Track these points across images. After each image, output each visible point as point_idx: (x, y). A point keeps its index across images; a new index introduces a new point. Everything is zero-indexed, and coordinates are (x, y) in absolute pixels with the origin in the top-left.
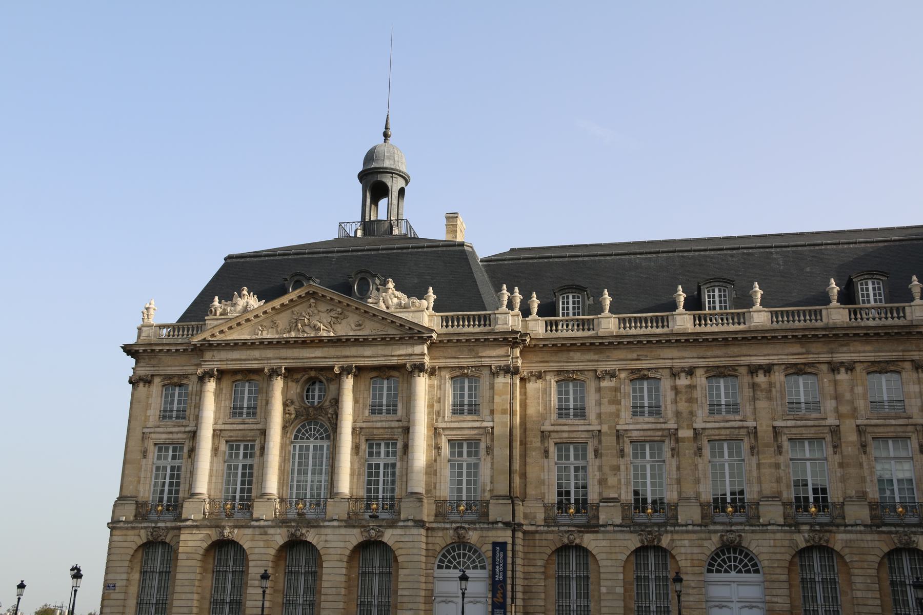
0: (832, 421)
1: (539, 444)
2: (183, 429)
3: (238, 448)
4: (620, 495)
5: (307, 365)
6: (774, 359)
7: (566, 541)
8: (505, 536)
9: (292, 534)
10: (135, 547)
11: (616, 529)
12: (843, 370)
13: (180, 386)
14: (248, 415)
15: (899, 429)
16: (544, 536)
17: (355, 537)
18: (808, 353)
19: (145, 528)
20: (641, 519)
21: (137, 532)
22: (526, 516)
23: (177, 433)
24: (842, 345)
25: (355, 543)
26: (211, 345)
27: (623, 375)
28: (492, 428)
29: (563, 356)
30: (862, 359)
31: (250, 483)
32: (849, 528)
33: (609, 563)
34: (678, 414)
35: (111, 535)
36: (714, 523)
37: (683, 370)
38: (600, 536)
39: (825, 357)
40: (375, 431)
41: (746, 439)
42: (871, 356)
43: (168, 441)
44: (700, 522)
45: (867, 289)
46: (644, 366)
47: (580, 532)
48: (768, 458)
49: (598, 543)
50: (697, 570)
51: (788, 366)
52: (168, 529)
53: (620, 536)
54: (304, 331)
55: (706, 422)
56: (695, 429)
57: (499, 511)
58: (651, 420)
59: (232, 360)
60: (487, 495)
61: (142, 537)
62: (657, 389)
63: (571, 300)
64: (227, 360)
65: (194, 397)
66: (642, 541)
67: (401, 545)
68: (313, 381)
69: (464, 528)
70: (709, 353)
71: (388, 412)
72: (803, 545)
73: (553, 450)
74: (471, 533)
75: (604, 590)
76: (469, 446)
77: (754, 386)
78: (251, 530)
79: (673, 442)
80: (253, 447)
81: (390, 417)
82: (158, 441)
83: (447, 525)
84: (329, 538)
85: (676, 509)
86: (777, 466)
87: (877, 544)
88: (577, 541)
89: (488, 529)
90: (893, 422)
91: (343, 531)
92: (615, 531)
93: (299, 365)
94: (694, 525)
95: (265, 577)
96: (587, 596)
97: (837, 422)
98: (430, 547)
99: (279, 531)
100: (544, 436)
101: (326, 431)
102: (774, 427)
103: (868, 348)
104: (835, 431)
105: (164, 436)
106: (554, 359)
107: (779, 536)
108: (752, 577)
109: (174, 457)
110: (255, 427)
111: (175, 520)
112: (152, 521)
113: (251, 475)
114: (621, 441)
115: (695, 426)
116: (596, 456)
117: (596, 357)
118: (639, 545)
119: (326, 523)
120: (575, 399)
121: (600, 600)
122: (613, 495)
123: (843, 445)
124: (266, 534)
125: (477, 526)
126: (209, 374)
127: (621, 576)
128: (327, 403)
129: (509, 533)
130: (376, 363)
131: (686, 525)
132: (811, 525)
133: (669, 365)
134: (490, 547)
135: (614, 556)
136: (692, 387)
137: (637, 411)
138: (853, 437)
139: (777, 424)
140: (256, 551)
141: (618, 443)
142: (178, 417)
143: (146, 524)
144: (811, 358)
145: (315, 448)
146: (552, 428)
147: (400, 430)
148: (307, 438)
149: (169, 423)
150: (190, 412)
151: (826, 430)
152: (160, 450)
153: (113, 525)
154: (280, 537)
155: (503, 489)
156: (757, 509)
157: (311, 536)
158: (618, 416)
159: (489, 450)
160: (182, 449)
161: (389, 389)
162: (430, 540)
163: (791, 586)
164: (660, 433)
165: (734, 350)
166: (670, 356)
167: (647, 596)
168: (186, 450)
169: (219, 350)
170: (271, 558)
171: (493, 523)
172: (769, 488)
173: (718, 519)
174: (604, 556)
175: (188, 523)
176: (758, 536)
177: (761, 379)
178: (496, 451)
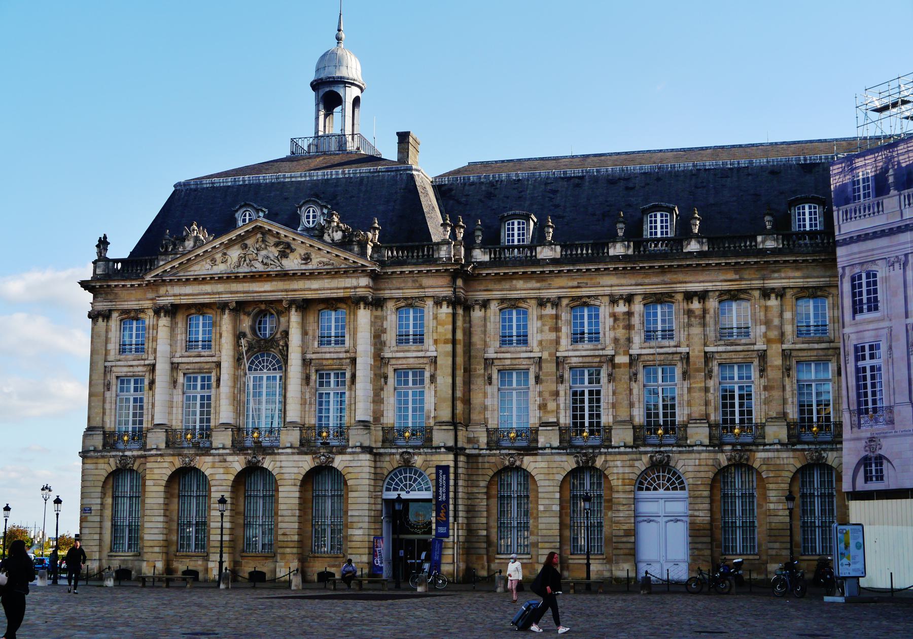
0: (760, 346)
1: (482, 371)
2: (142, 362)
3: (195, 379)
4: (558, 420)
5: (256, 299)
6: (708, 286)
7: (507, 463)
8: (448, 460)
9: (249, 462)
10: (106, 475)
11: (554, 451)
12: (773, 296)
13: (137, 319)
14: (204, 347)
15: (821, 353)
16: (486, 459)
17: (307, 463)
18: (741, 279)
19: (114, 456)
20: (579, 442)
21: (106, 460)
22: (469, 440)
23: (137, 366)
24: (774, 272)
25: (308, 469)
28: (436, 357)
29: (506, 285)
30: (791, 285)
31: (209, 413)
32: (768, 447)
33: (547, 483)
34: (616, 340)
35: (83, 463)
36: (645, 445)
37: (621, 297)
38: (539, 458)
39: (757, 283)
40: (325, 362)
41: (679, 364)
42: (800, 282)
43: (129, 374)
44: (632, 444)
45: (804, 214)
46: (584, 294)
47: (519, 454)
48: (698, 382)
49: (537, 465)
50: (628, 488)
51: (722, 293)
52: (135, 458)
53: (557, 458)
55: (641, 348)
56: (631, 355)
57: (442, 437)
58: (590, 346)
59: (186, 295)
60: (432, 422)
61: (113, 465)
62: (597, 316)
63: (516, 226)
64: (180, 295)
65: (151, 331)
66: (577, 462)
67: (350, 470)
68: (262, 314)
69: (409, 453)
70: (647, 281)
71: (337, 343)
72: (725, 463)
73: (495, 376)
74: (416, 457)
75: (541, 508)
76: (414, 375)
77: (690, 313)
79: (610, 369)
80: (209, 379)
81: (338, 348)
82: (119, 374)
83: (393, 451)
84: (283, 464)
85: (610, 432)
86: (706, 390)
87: (792, 461)
88: (518, 463)
89: (432, 454)
90: (816, 346)
91: (296, 457)
92: (552, 454)
93: (248, 297)
94: (625, 446)
95: (222, 501)
96: (526, 513)
97: (764, 347)
98: (379, 471)
99: (236, 458)
100: (489, 363)
101: (278, 362)
102: (706, 353)
103: (797, 274)
104: (763, 356)
105: (126, 369)
106: (497, 287)
107: (703, 455)
108: (679, 493)
109: (136, 390)
110: (210, 359)
111: (140, 449)
112: (119, 450)
113: (209, 406)
114: (561, 367)
115: (631, 352)
116: (537, 382)
117: (538, 285)
118: (575, 466)
119: (280, 451)
120: (518, 327)
121: (537, 518)
122: (551, 420)
123: (769, 369)
125: (422, 450)
127: (558, 495)
128: (278, 336)
129: (451, 457)
130: (322, 296)
131: (619, 447)
132: (733, 445)
133: (608, 292)
134: (434, 470)
135: (551, 477)
136: (630, 314)
137: (578, 338)
138: (778, 362)
139: (707, 349)
140: (217, 477)
141: (557, 369)
142: (137, 350)
143: (114, 453)
144: (744, 285)
145: (268, 378)
146: (494, 356)
147: (348, 361)
148: (261, 370)
149: (130, 357)
150: (148, 346)
151: (755, 355)
152: (122, 382)
153: (84, 454)
155: (446, 415)
156: (685, 431)
157: (268, 463)
158: (558, 342)
159: (433, 378)
160: (142, 381)
161: (337, 320)
162: (379, 464)
163: (712, 503)
164: (598, 360)
165: (668, 277)
166: (609, 283)
168: (146, 382)
169: (172, 286)
170: (230, 483)
171: (436, 448)
172: (698, 410)
173: (651, 441)
174: (542, 477)
176: (685, 456)
177: (696, 305)
178: (440, 380)
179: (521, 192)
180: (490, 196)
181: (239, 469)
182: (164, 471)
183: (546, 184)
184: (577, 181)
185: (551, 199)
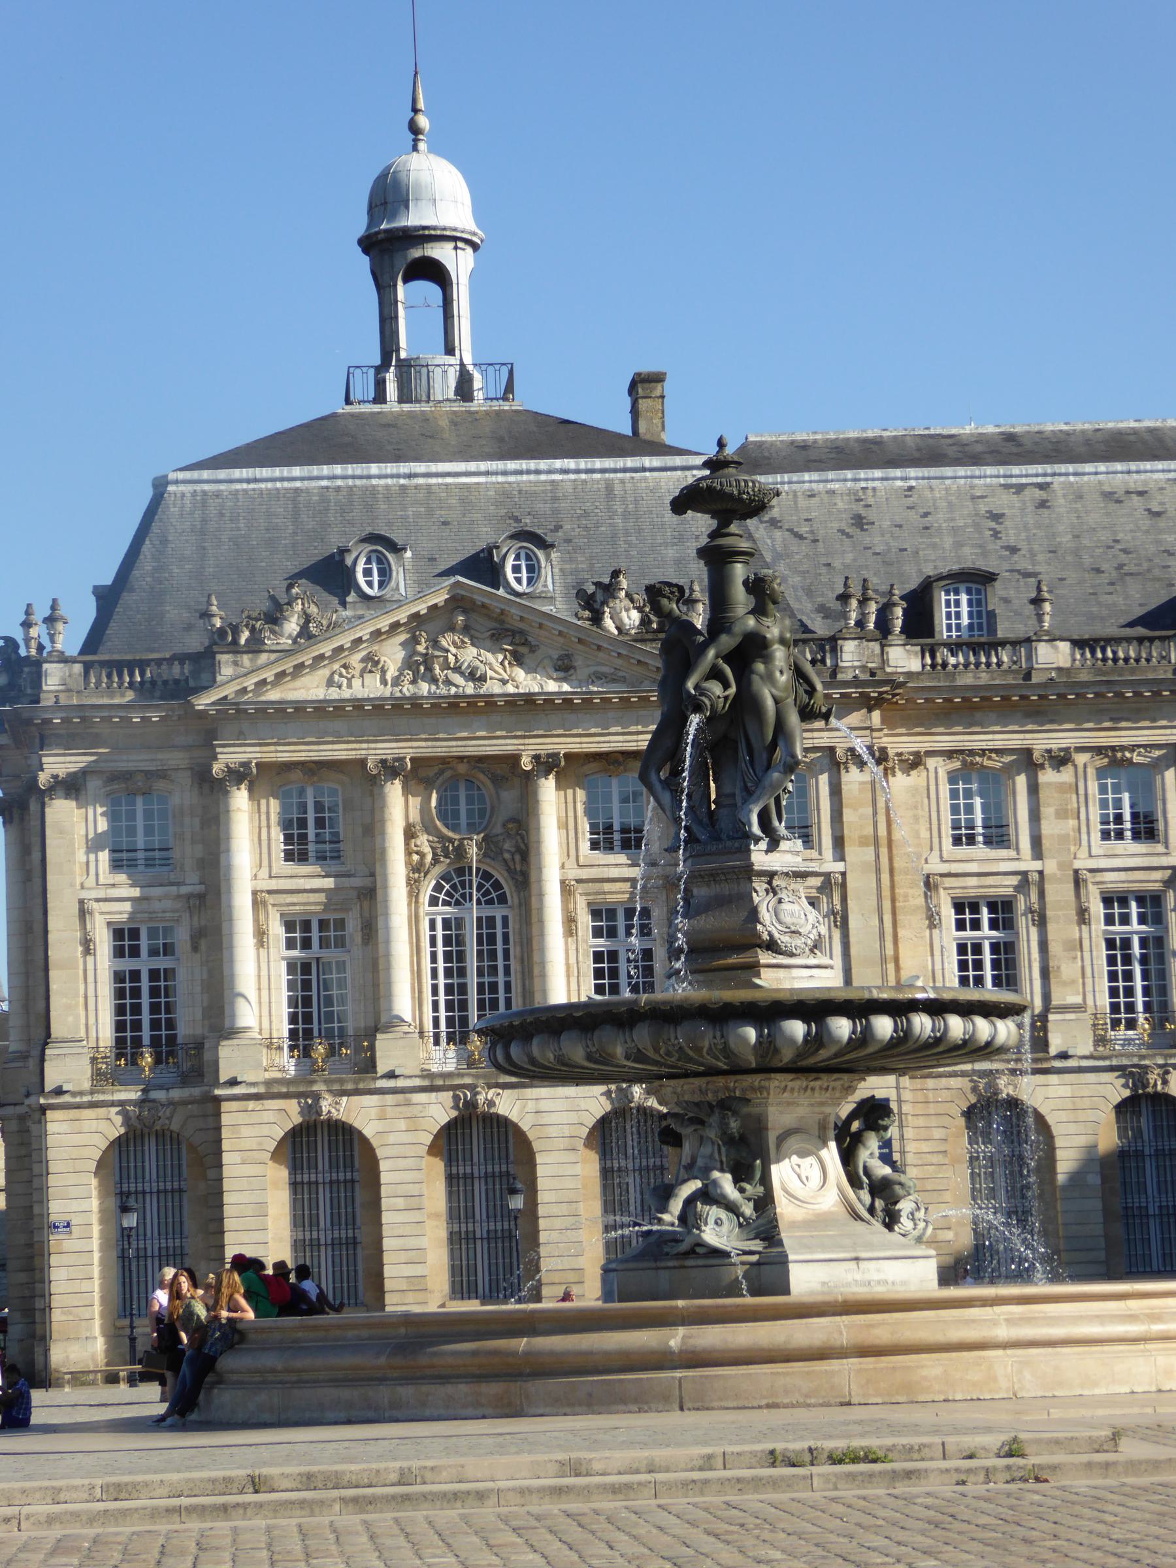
21: (101, 1111)
26: (240, 712)
27: (1081, 759)
28: (844, 874)
33: (1072, 1128)
46: (1126, 741)
49: (1052, 1092)
54: (448, 682)
78: (375, 1097)
84: (544, 1105)
124: (408, 1104)
126: (238, 775)
130: (605, 748)
135: (1081, 1115)
140: (392, 1138)
150: (187, 853)
154: (438, 1110)
167: (1142, 1188)
174: (1063, 1116)
175: (237, 1090)
179: (926, 515)
180: (859, 522)
181: (444, 1119)
182: (265, 1130)
183: (974, 498)
184: (1038, 494)
185: (996, 534)
